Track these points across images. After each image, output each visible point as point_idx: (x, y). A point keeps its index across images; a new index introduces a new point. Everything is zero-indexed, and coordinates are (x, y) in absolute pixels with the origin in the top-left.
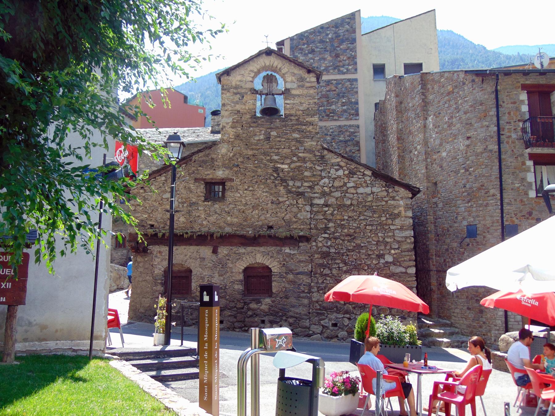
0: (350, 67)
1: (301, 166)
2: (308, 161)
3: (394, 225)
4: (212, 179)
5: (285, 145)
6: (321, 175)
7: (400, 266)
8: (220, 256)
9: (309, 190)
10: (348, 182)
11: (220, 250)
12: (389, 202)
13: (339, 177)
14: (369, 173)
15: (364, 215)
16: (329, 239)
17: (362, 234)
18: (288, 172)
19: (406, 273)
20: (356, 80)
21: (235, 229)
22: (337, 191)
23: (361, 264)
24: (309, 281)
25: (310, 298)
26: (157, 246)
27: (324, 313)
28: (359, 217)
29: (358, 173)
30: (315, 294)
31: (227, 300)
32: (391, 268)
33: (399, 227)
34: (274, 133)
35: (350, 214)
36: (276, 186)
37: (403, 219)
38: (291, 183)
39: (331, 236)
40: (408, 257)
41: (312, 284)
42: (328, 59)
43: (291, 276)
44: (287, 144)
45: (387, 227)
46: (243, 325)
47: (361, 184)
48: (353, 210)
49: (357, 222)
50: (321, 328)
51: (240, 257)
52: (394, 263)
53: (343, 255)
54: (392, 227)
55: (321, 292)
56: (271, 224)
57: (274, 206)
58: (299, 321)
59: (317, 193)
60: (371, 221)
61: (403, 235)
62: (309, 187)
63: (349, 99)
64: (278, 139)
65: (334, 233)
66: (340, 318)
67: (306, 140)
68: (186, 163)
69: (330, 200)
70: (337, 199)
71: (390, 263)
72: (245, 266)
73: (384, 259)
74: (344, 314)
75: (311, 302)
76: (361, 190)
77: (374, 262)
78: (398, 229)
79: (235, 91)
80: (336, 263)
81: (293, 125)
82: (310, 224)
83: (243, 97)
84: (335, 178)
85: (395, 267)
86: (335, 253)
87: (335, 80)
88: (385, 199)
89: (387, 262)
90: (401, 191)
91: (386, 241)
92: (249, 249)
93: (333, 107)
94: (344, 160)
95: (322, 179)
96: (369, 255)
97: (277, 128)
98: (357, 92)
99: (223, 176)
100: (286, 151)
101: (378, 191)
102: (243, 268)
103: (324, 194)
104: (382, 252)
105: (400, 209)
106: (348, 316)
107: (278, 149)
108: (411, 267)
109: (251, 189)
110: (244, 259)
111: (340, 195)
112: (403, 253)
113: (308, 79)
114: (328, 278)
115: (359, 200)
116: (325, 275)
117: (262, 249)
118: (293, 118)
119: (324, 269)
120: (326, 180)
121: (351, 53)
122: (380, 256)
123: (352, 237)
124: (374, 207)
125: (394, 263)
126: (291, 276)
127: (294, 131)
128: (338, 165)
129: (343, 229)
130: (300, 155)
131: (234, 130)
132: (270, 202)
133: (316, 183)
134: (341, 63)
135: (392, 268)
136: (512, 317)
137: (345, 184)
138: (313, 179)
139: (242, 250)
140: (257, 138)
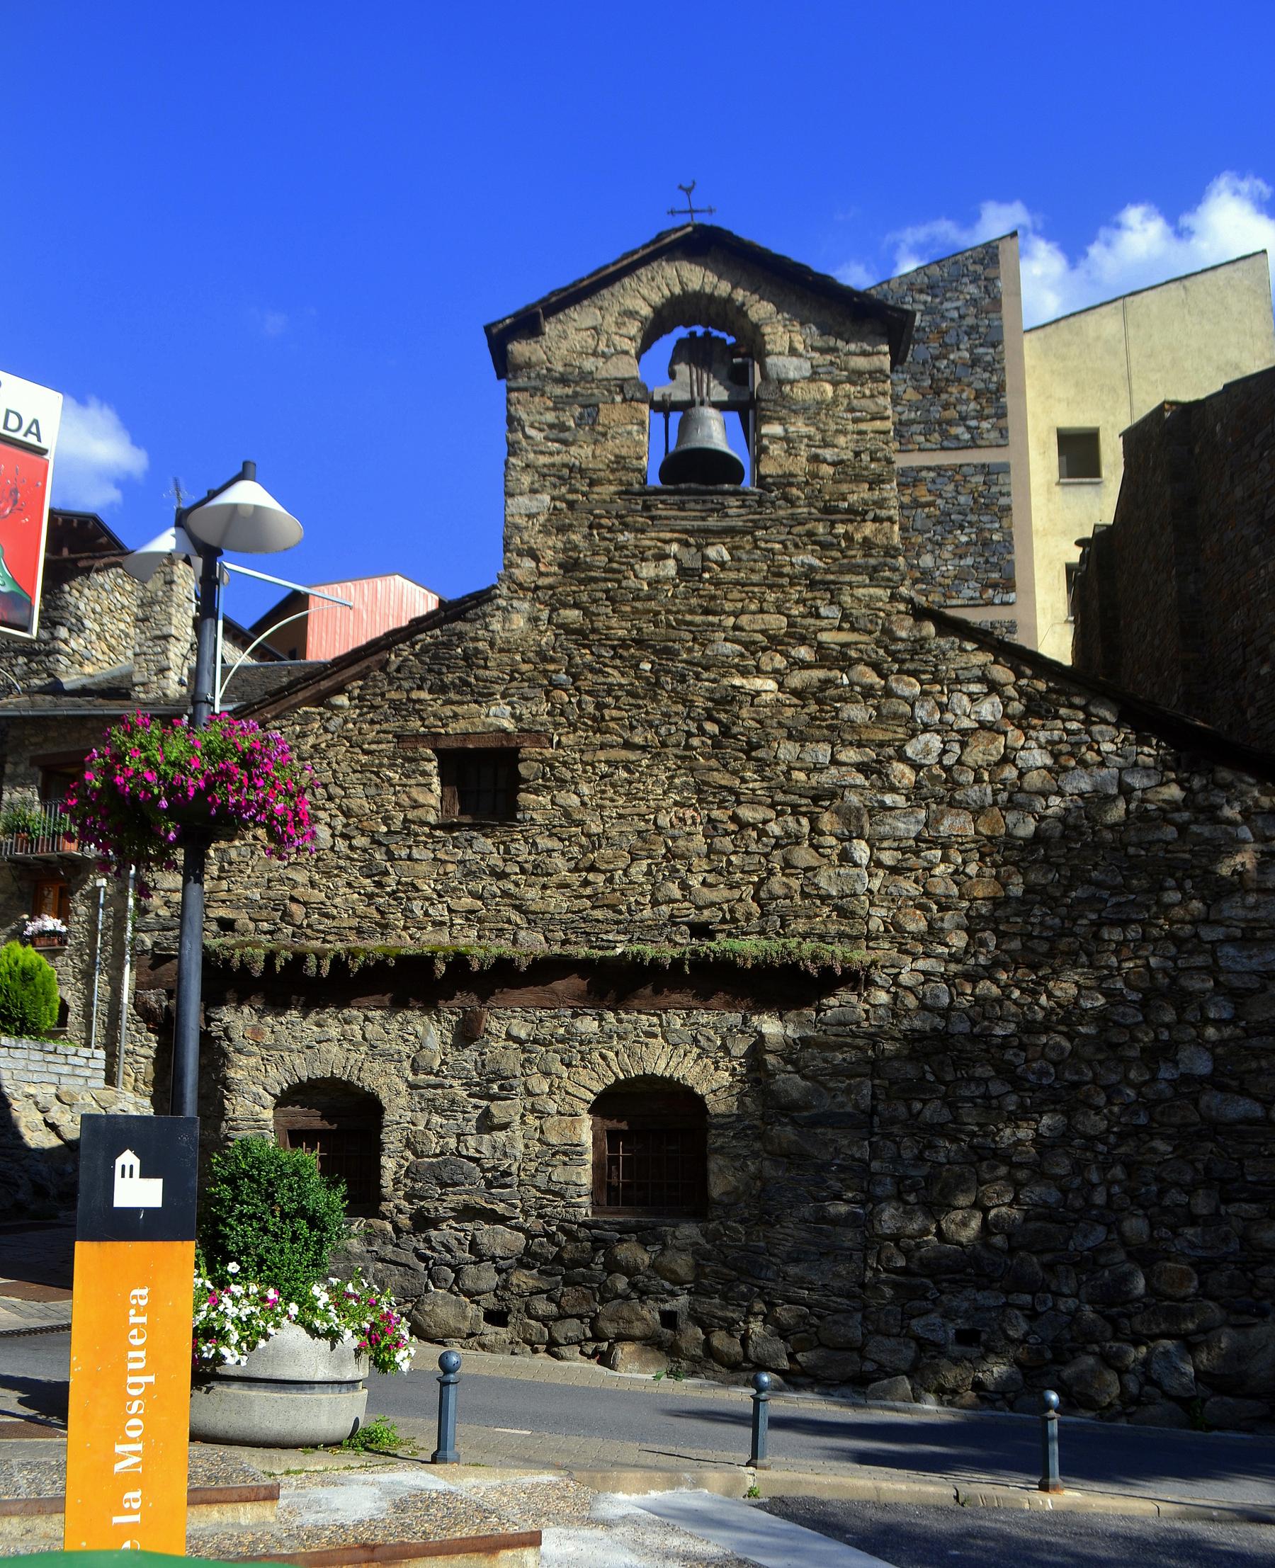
0: (985, 425)
5: (762, 600)
7: (1243, 1092)
9: (860, 779)
10: (1023, 748)
12: (1194, 828)
15: (1090, 882)
20: (1004, 469)
23: (1075, 1085)
27: (926, 1289)
28: (1070, 887)
32: (1205, 1100)
33: (1238, 933)
34: (718, 552)
35: (1034, 877)
37: (1251, 899)
38: (787, 751)
42: (907, 396)
43: (785, 1133)
44: (771, 597)
48: (1046, 859)
49: (1063, 911)
50: (909, 1353)
52: (1214, 1081)
55: (912, 1198)
60: (1118, 904)
61: (1255, 964)
62: (862, 768)
63: (981, 530)
64: (733, 575)
66: (989, 1309)
67: (847, 578)
69: (947, 822)
71: (1202, 1080)
73: (1176, 1063)
74: (1008, 1293)
77: (1132, 1075)
78: (1230, 940)
80: (972, 1079)
85: (1220, 1096)
87: (929, 469)
88: (1176, 816)
89: (1187, 1078)
91: (1182, 989)
93: (927, 561)
95: (913, 735)
96: (1114, 1046)
97: (731, 531)
98: (1008, 509)
100: (761, 621)
104: (1165, 1035)
107: (736, 615)
112: (1254, 1042)
116: (932, 1126)
119: (925, 1102)
121: (986, 375)
122: (1161, 1052)
124: (1131, 850)
125: (1214, 1081)
128: (982, 679)
130: (824, 637)
134: (952, 414)
138: (880, 736)
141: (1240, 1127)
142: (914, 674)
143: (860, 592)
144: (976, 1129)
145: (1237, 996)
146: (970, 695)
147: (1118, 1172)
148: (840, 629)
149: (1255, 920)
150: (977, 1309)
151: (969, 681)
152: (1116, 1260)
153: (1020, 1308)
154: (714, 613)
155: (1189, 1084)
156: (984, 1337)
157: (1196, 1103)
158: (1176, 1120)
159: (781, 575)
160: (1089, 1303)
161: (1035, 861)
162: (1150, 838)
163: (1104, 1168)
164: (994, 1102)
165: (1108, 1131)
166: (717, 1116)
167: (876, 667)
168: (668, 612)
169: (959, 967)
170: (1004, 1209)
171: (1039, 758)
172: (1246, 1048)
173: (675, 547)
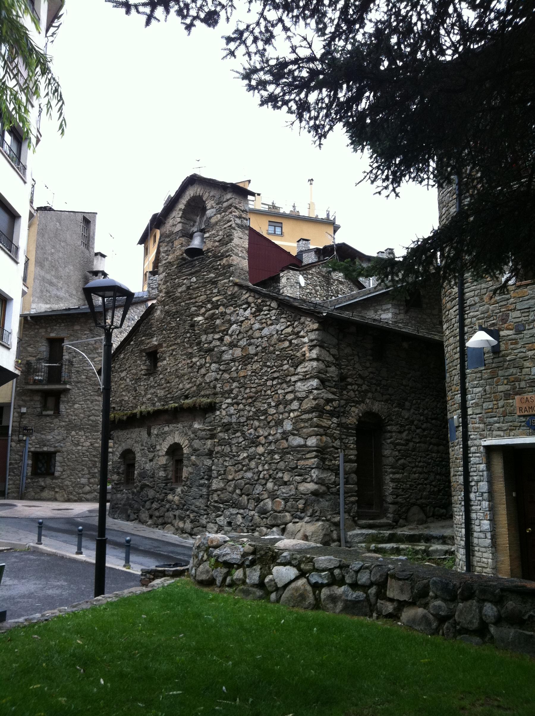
1: (214, 314)
2: (220, 305)
3: (297, 374)
4: (150, 348)
6: (230, 320)
8: (153, 437)
9: (218, 343)
11: (152, 431)
13: (247, 318)
14: (274, 304)
16: (232, 404)
17: (263, 393)
18: (203, 324)
19: (305, 446)
21: (163, 403)
22: (244, 337)
24: (208, 462)
25: (209, 486)
26: (117, 431)
27: (221, 508)
28: (261, 369)
29: (265, 308)
30: (215, 481)
31: (155, 490)
33: (301, 377)
36: (191, 346)
38: (203, 338)
39: (234, 401)
40: (309, 422)
41: (213, 467)
45: (289, 378)
46: (163, 521)
47: (266, 323)
51: (163, 435)
53: (243, 426)
54: (293, 379)
55: (220, 478)
56: (187, 392)
57: (190, 370)
58: (199, 517)
59: (225, 345)
60: (272, 373)
64: (196, 286)
65: (235, 397)
68: (135, 335)
69: (236, 353)
70: (243, 349)
72: (167, 447)
75: (211, 492)
76: (266, 332)
78: (300, 380)
79: (168, 240)
81: (211, 263)
82: (215, 387)
83: (173, 245)
84: (242, 322)
86: (236, 423)
89: (284, 433)
90: (307, 323)
92: (172, 426)
94: (252, 294)
95: (231, 325)
99: (156, 343)
101: (282, 328)
102: (166, 450)
103: (232, 345)
105: (304, 349)
106: (242, 511)
107: (196, 298)
108: (311, 436)
109: (174, 353)
110: (167, 438)
111: (245, 343)
113: (225, 200)
114: (227, 459)
115: (263, 346)
117: (180, 425)
118: (210, 254)
119: (225, 445)
120: (234, 326)
123: (254, 399)
124: (277, 353)
126: (193, 458)
127: (210, 272)
129: (246, 388)
131: (165, 287)
132: (186, 366)
133: (225, 333)
135: (291, 438)
136: (477, 522)
137: (251, 328)
138: (223, 328)
139: (166, 429)
140: (180, 290)
141: (298, 448)
142: (232, 305)
143: (223, 282)
144: (235, 454)
145: (300, 400)
146: (243, 309)
147: (266, 467)
148: (217, 296)
149: (306, 372)
150: (231, 514)
151: (244, 304)
152: (265, 498)
153: (241, 514)
154: (192, 299)
155: (285, 436)
156: (232, 524)
157: (287, 440)
158: (281, 447)
159: (205, 282)
160: (258, 513)
161: (254, 362)
162: (281, 347)
163: (264, 465)
164: (240, 445)
165: (264, 453)
166: (185, 454)
167: (223, 305)
168: (184, 301)
169: (234, 401)
170: (240, 481)
171: (257, 326)
172: (301, 419)
173: (185, 281)
